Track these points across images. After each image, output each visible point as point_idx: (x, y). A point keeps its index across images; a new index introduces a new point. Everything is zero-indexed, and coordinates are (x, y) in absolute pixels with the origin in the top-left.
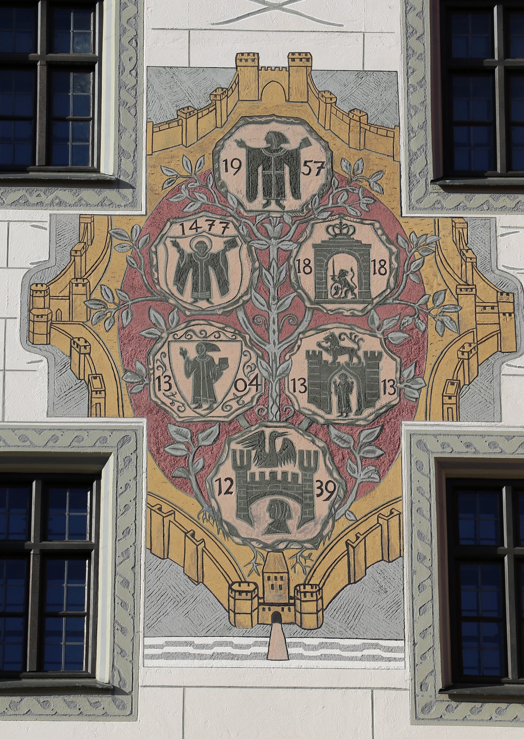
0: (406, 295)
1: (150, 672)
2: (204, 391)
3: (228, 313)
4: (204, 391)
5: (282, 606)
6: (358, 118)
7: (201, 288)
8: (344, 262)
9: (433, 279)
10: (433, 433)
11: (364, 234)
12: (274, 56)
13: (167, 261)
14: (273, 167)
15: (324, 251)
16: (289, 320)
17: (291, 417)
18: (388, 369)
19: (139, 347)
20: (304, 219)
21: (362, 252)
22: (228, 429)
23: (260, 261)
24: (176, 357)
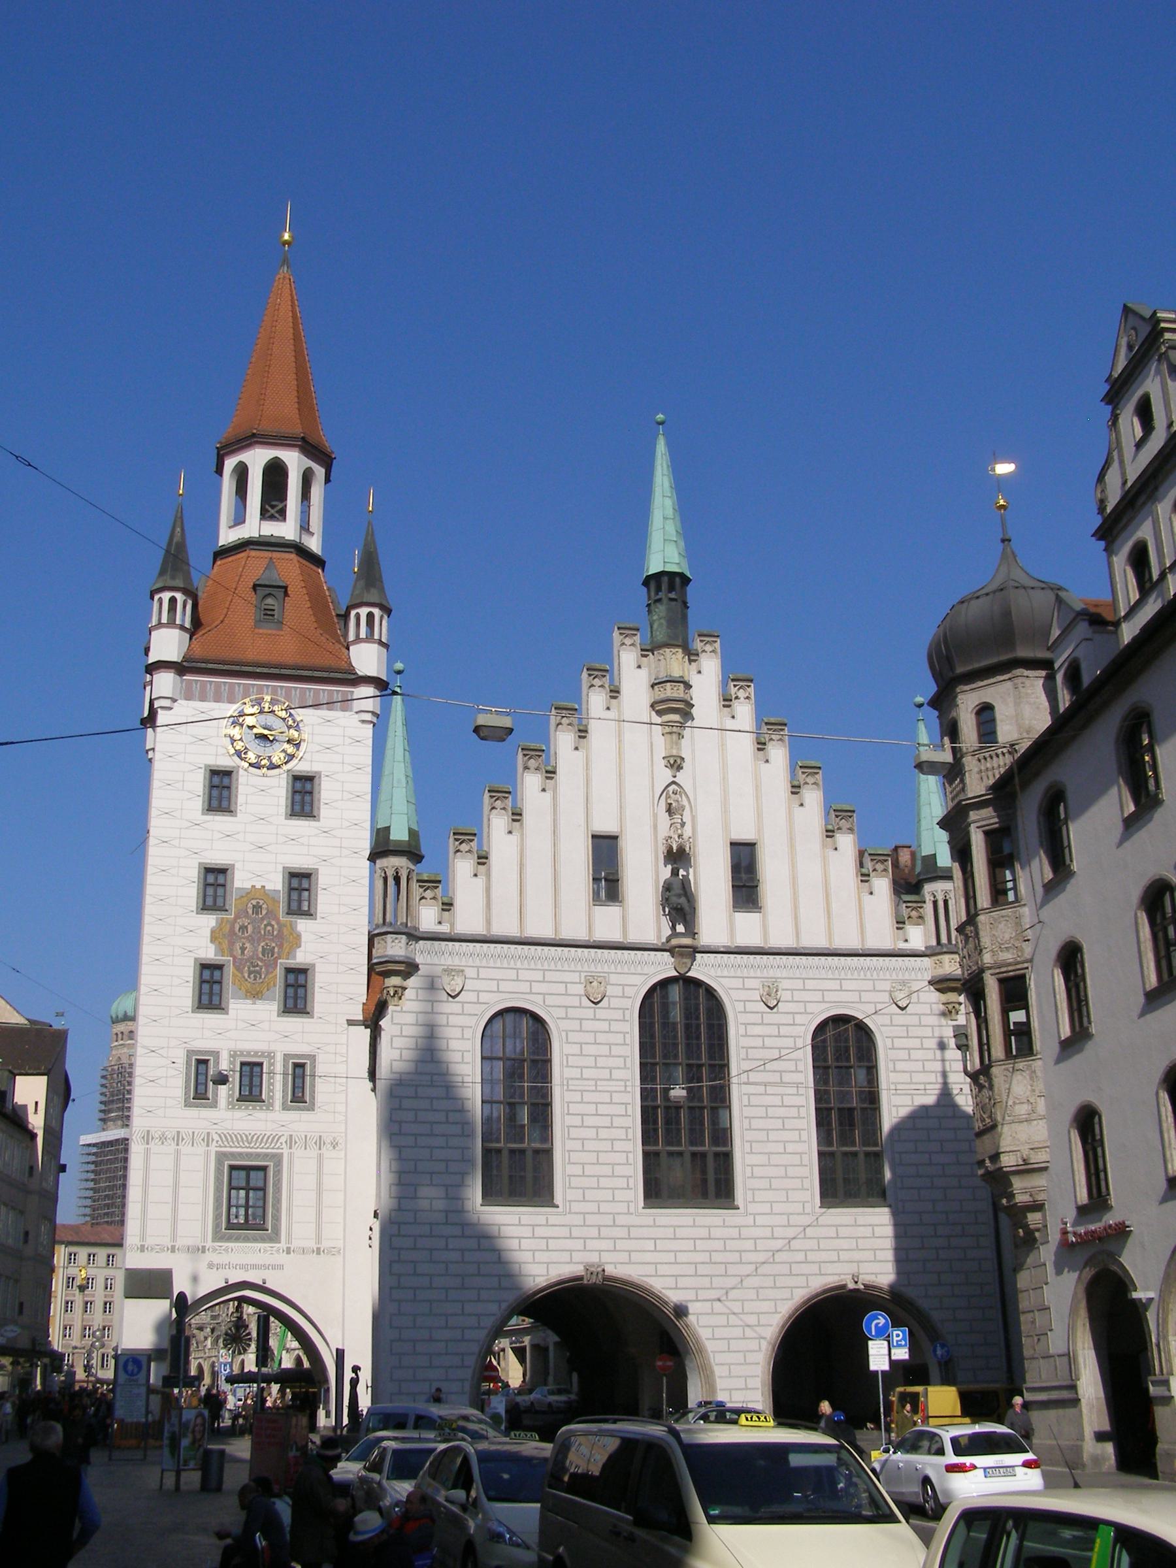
0: (280, 935)
1: (231, 1006)
2: (243, 953)
3: (247, 938)
4: (243, 953)
5: (255, 995)
6: (273, 899)
8: (269, 928)
9: (285, 932)
10: (283, 962)
11: (273, 923)
12: (258, 886)
14: (257, 908)
17: (259, 959)
19: (232, 944)
20: (263, 919)
22: (247, 960)
24: (238, 946)
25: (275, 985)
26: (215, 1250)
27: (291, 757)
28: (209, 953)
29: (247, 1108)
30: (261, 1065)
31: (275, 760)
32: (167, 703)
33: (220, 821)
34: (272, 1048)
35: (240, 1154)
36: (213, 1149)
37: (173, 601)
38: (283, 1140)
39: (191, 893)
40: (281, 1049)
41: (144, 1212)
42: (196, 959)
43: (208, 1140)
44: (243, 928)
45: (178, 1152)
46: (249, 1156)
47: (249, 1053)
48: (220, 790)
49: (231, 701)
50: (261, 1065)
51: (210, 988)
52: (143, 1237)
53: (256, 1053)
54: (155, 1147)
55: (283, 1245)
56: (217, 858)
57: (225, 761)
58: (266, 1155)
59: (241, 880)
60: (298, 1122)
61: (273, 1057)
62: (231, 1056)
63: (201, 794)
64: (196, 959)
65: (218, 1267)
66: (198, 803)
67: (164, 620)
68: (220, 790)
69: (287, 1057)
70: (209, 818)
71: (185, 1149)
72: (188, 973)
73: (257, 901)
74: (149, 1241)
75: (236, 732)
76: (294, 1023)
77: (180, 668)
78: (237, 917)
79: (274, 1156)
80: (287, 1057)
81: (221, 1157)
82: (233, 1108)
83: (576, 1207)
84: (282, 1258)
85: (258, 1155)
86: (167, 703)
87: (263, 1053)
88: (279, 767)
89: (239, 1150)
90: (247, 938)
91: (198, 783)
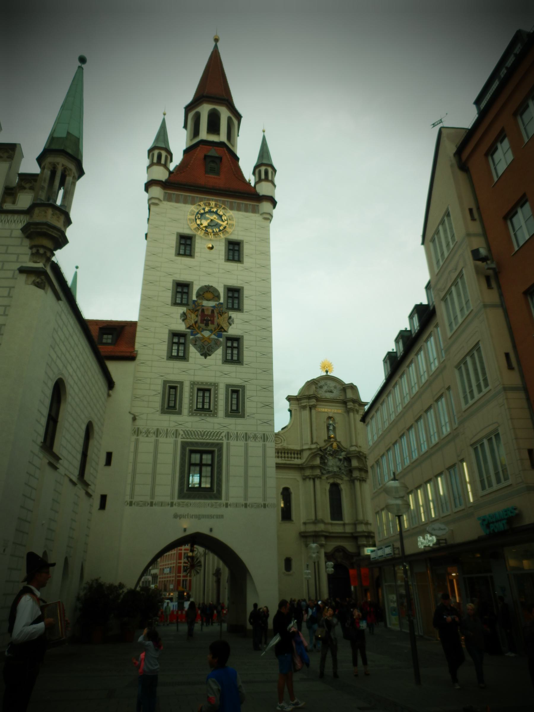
26: (179, 504)
29: (201, 415)
30: (209, 390)
32: (156, 201)
33: (186, 260)
34: (217, 380)
35: (197, 443)
36: (180, 440)
37: (159, 157)
38: (223, 434)
39: (168, 295)
42: (170, 331)
45: (157, 442)
46: (202, 444)
47: (202, 383)
48: (185, 244)
49: (193, 203)
50: (209, 390)
52: (132, 495)
53: (207, 384)
55: (223, 501)
56: (184, 277)
58: (212, 444)
61: (217, 386)
64: (170, 331)
65: (181, 517)
66: (173, 251)
67: (155, 160)
68: (185, 244)
70: (179, 258)
71: (162, 439)
72: (165, 337)
74: (136, 499)
76: (229, 368)
77: (165, 185)
81: (184, 445)
82: (192, 415)
84: (221, 511)
85: (208, 444)
86: (156, 201)
91: (173, 241)
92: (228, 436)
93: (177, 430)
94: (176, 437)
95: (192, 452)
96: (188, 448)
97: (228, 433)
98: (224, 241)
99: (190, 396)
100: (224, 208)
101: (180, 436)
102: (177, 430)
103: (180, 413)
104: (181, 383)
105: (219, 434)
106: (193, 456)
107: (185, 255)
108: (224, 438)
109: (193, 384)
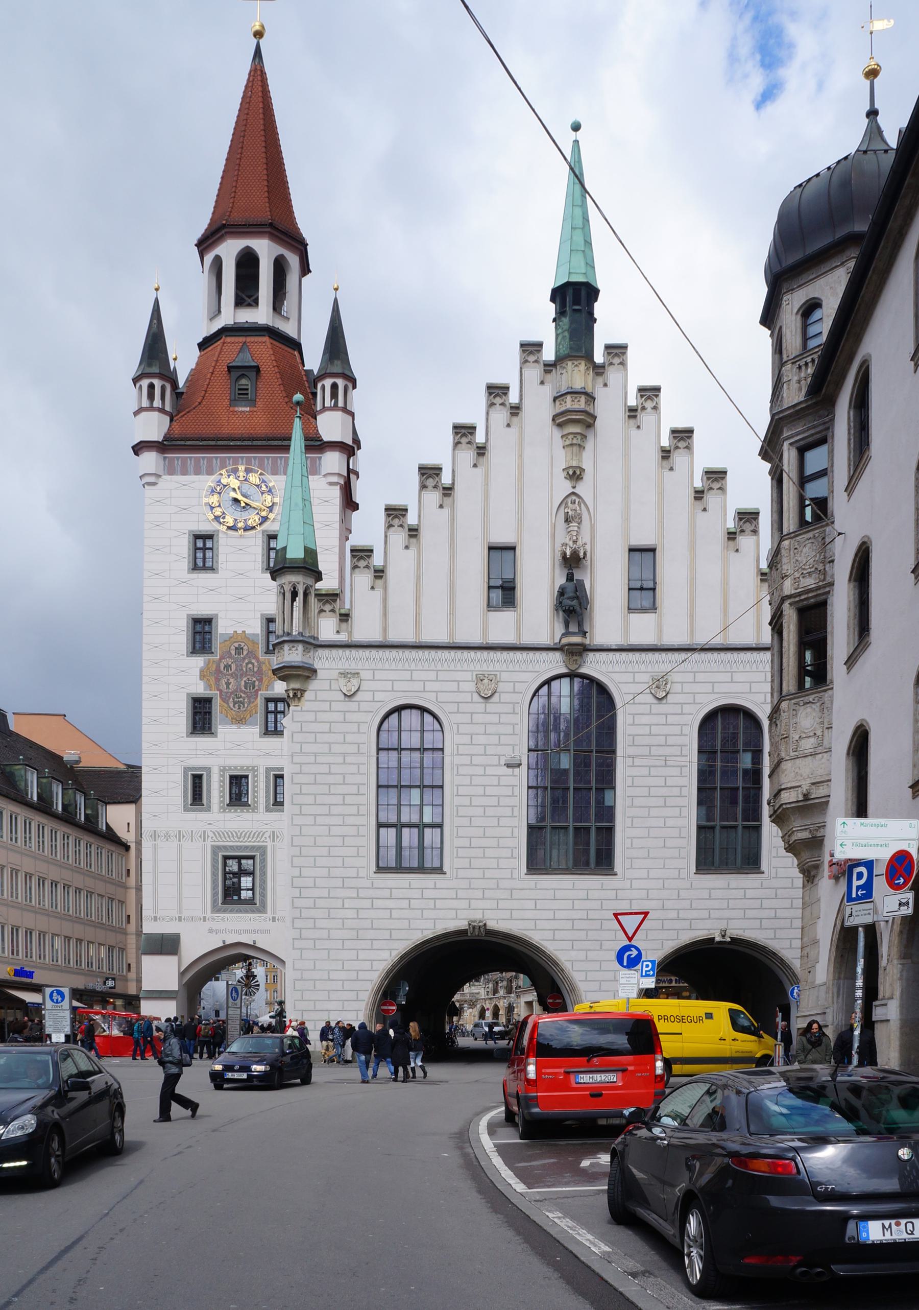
1: (219, 731)
2: (228, 687)
3: (231, 675)
4: (228, 687)
5: (240, 721)
7: (227, 670)
8: (250, 666)
9: (264, 668)
11: (253, 661)
12: (239, 631)
13: (222, 666)
14: (239, 650)
15: (247, 664)
16: (242, 675)
17: (242, 691)
18: (257, 683)
19: (218, 680)
20: (244, 659)
21: (253, 664)
22: (232, 693)
23: (237, 666)
24: (223, 681)
25: (256, 713)
27: (265, 519)
28: (200, 689)
29: (236, 811)
30: (247, 777)
31: (250, 523)
34: (255, 764)
35: (231, 847)
36: (209, 843)
38: (267, 835)
39: (182, 639)
40: (263, 764)
41: (155, 892)
42: (188, 694)
43: (204, 836)
44: (227, 667)
46: (239, 848)
47: (236, 768)
50: (247, 777)
51: (201, 717)
53: (242, 768)
54: (161, 843)
57: (205, 527)
58: (253, 847)
59: (223, 628)
60: (278, 821)
62: (221, 770)
63: (187, 556)
64: (188, 694)
66: (185, 564)
69: (268, 770)
73: (239, 646)
75: (214, 500)
78: (222, 658)
79: (260, 847)
80: (268, 770)
81: (215, 850)
83: (461, 873)
85: (247, 847)
87: (248, 768)
88: (253, 528)
89: (231, 844)
90: (231, 675)
91: (183, 547)
92: (274, 836)
93: (204, 832)
94: (204, 841)
95: (226, 858)
96: (220, 854)
97: (273, 832)
98: (261, 535)
99: (221, 786)
100: (261, 474)
101: (210, 839)
102: (204, 832)
103: (209, 809)
104: (208, 770)
105: (260, 834)
106: (230, 862)
107: (205, 568)
108: (268, 839)
109: (223, 770)
